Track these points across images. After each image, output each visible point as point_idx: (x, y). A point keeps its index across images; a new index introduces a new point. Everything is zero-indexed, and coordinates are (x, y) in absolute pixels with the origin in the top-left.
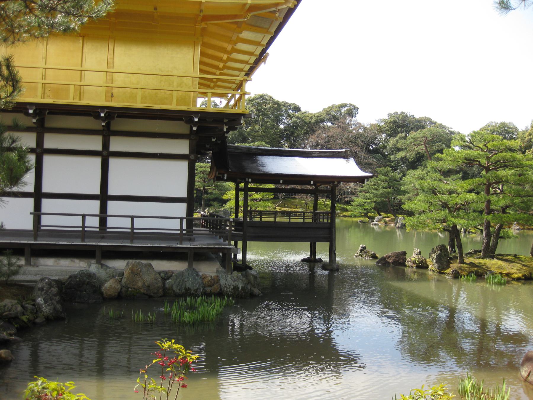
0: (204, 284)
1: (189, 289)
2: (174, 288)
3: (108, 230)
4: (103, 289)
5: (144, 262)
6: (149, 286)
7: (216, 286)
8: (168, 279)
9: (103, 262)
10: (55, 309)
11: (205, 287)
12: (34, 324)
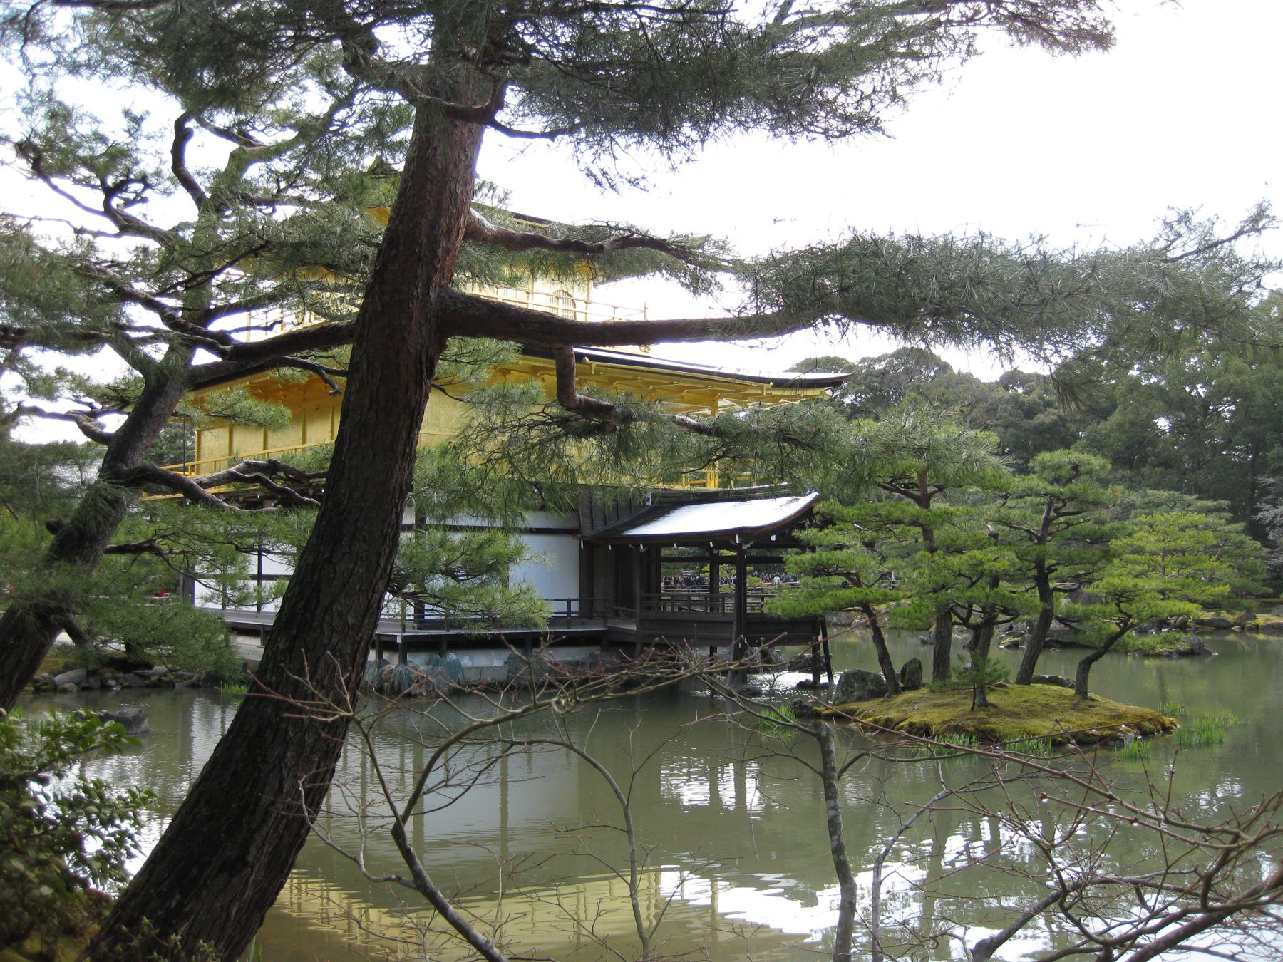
12: (174, 686)
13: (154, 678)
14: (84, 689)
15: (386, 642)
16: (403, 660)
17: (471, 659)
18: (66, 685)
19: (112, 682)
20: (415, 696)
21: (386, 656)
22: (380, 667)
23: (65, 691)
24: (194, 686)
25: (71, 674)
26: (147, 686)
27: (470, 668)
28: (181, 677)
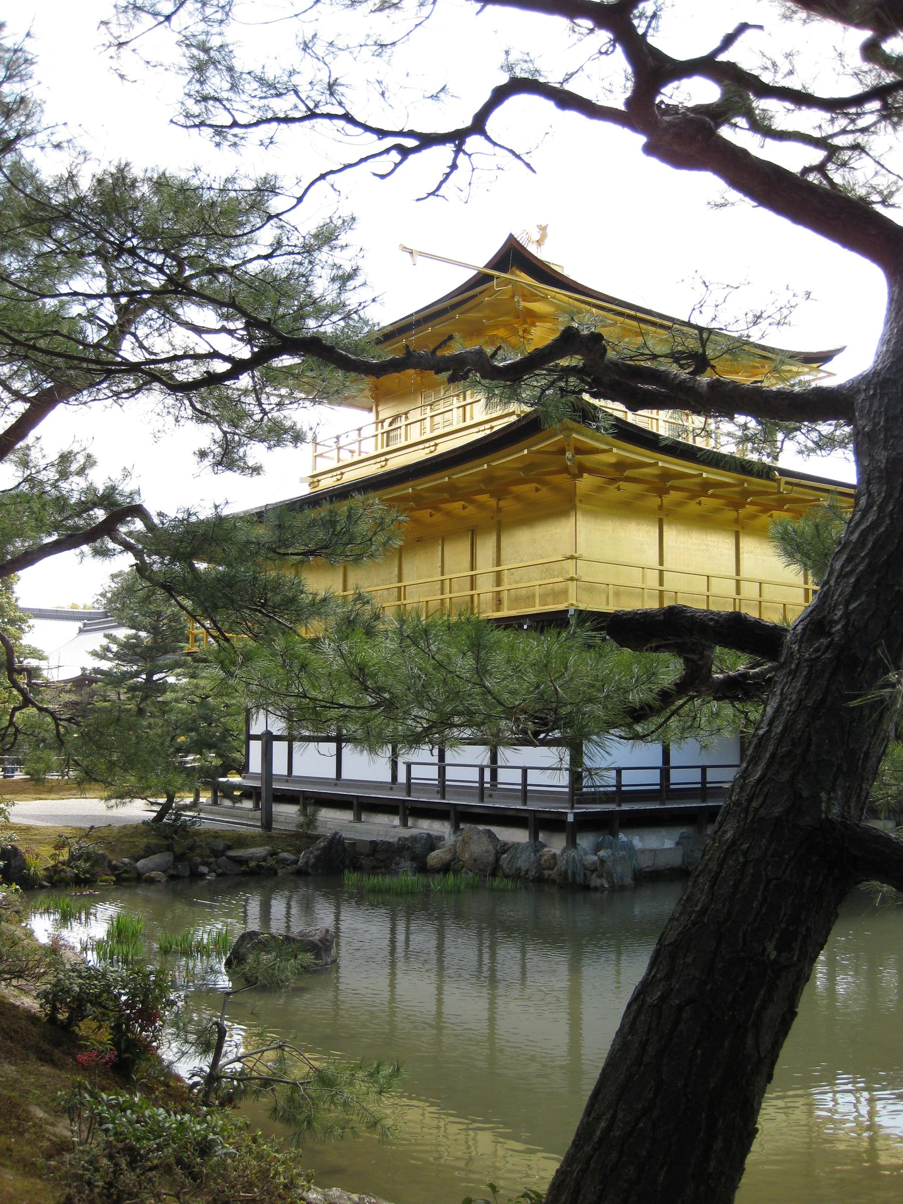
0: (540, 865)
1: (520, 869)
2: (505, 866)
3: (499, 786)
4: (429, 857)
5: (481, 827)
6: (475, 860)
7: (555, 870)
8: (504, 853)
9: (462, 826)
10: (307, 863)
11: (544, 869)
12: (276, 873)
13: (253, 864)
14: (172, 878)
15: (542, 820)
16: (572, 843)
17: (641, 839)
18: (153, 874)
19: (204, 869)
20: (596, 889)
21: (542, 837)
22: (536, 851)
23: (151, 881)
24: (301, 873)
25: (156, 859)
26: (244, 874)
27: (643, 851)
28: (284, 861)
